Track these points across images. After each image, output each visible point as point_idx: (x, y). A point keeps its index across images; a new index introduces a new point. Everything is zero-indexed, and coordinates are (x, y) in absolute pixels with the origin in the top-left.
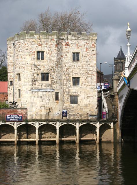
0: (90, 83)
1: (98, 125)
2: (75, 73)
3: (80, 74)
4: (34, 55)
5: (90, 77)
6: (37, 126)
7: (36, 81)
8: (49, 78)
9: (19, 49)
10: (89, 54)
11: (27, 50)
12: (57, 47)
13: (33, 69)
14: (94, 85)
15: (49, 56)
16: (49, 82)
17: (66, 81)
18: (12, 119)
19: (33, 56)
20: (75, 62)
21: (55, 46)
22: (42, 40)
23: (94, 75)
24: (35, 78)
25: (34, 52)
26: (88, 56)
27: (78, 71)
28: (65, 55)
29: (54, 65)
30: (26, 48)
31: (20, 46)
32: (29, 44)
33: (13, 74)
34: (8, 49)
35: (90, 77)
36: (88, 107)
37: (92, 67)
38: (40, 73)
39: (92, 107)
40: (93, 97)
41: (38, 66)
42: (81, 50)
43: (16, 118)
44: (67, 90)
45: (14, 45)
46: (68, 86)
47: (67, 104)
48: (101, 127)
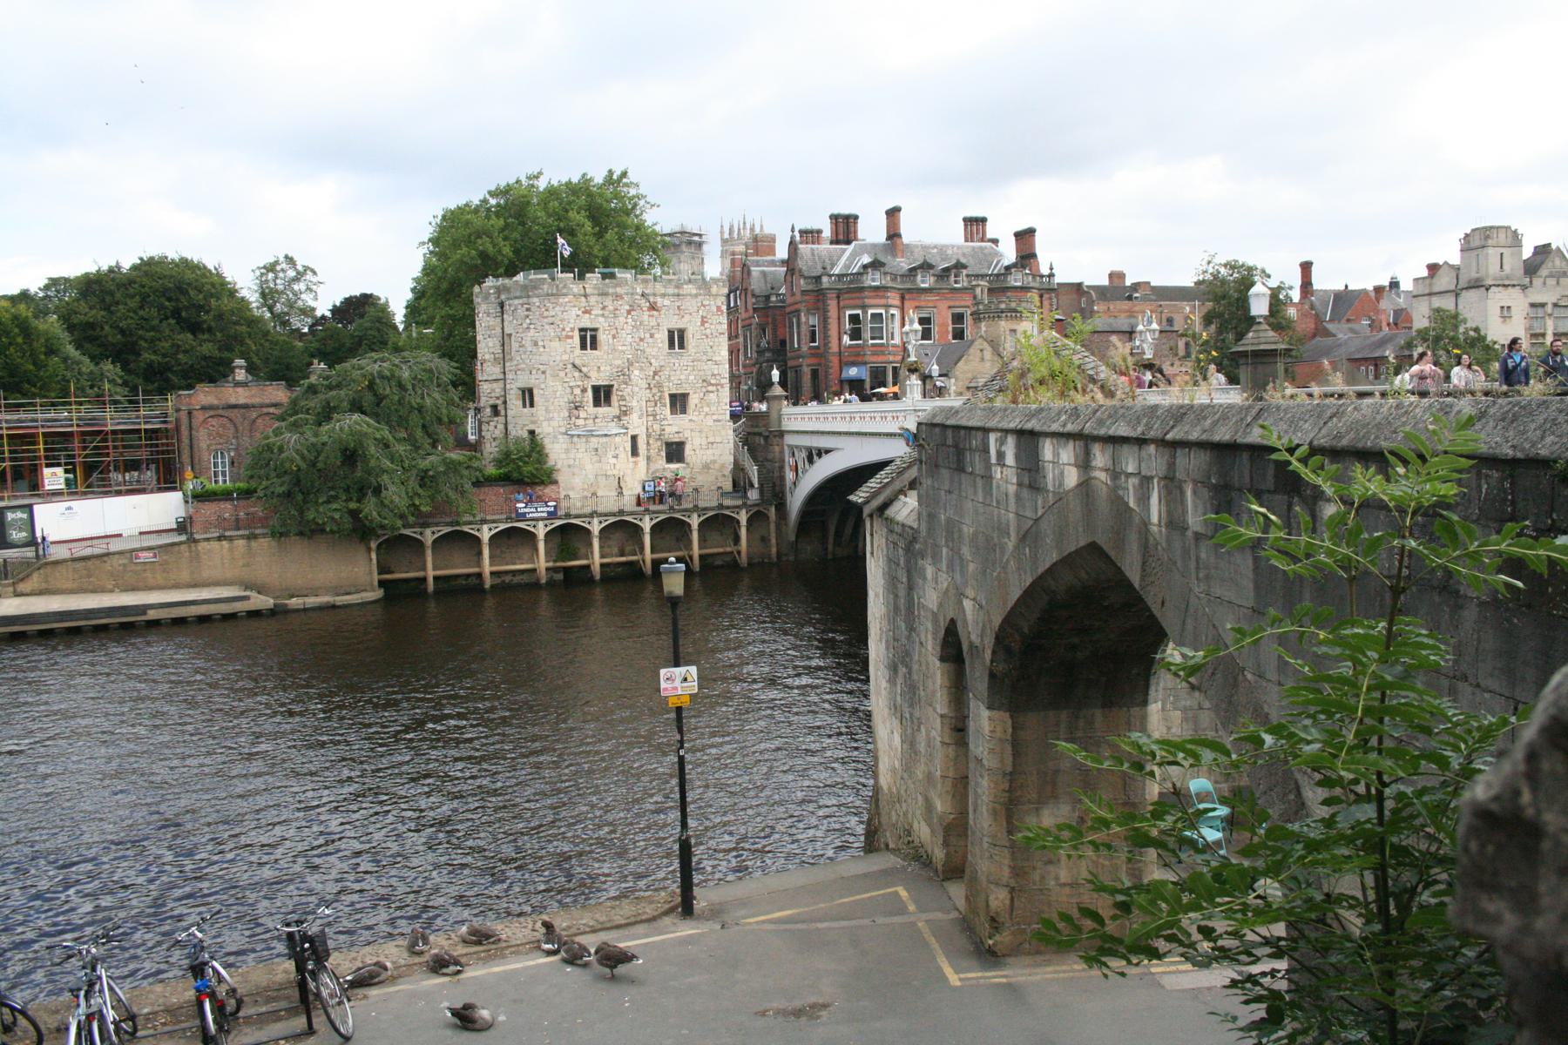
1: (743, 517)
6: (595, 527)
8: (614, 398)
16: (613, 410)
22: (593, 300)
25: (572, 330)
33: (501, 384)
44: (657, 427)
47: (661, 463)
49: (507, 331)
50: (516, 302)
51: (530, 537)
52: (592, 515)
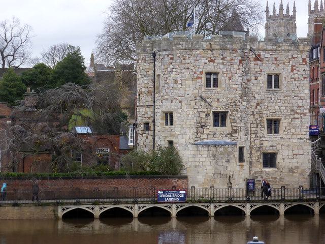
0: (298, 130)
2: (272, 111)
3: (280, 113)
4: (200, 78)
5: (298, 118)
6: (212, 210)
7: (204, 126)
8: (228, 121)
9: (171, 66)
10: (296, 76)
11: (188, 69)
12: (241, 64)
13: (198, 104)
14: (305, 133)
15: (227, 81)
16: (227, 129)
17: (255, 126)
18: (169, 197)
19: (199, 81)
20: (271, 92)
21: (238, 63)
22: (215, 52)
23: (305, 114)
24: (203, 121)
25: (201, 73)
26: (295, 80)
27: (277, 108)
28: (253, 78)
29: (236, 97)
30: (187, 66)
31: (174, 61)
32: (191, 58)
34: (140, 61)
35: (298, 118)
36: (294, 174)
37: (301, 101)
38: (212, 112)
39: (301, 174)
40: (303, 154)
41: (207, 100)
42: (283, 69)
43: (175, 196)
44: (257, 142)
45: (154, 57)
46: (258, 135)
47: (259, 167)
48: (321, 211)
49: (157, 73)
50: (164, 53)
51: (167, 215)
52: (211, 201)
